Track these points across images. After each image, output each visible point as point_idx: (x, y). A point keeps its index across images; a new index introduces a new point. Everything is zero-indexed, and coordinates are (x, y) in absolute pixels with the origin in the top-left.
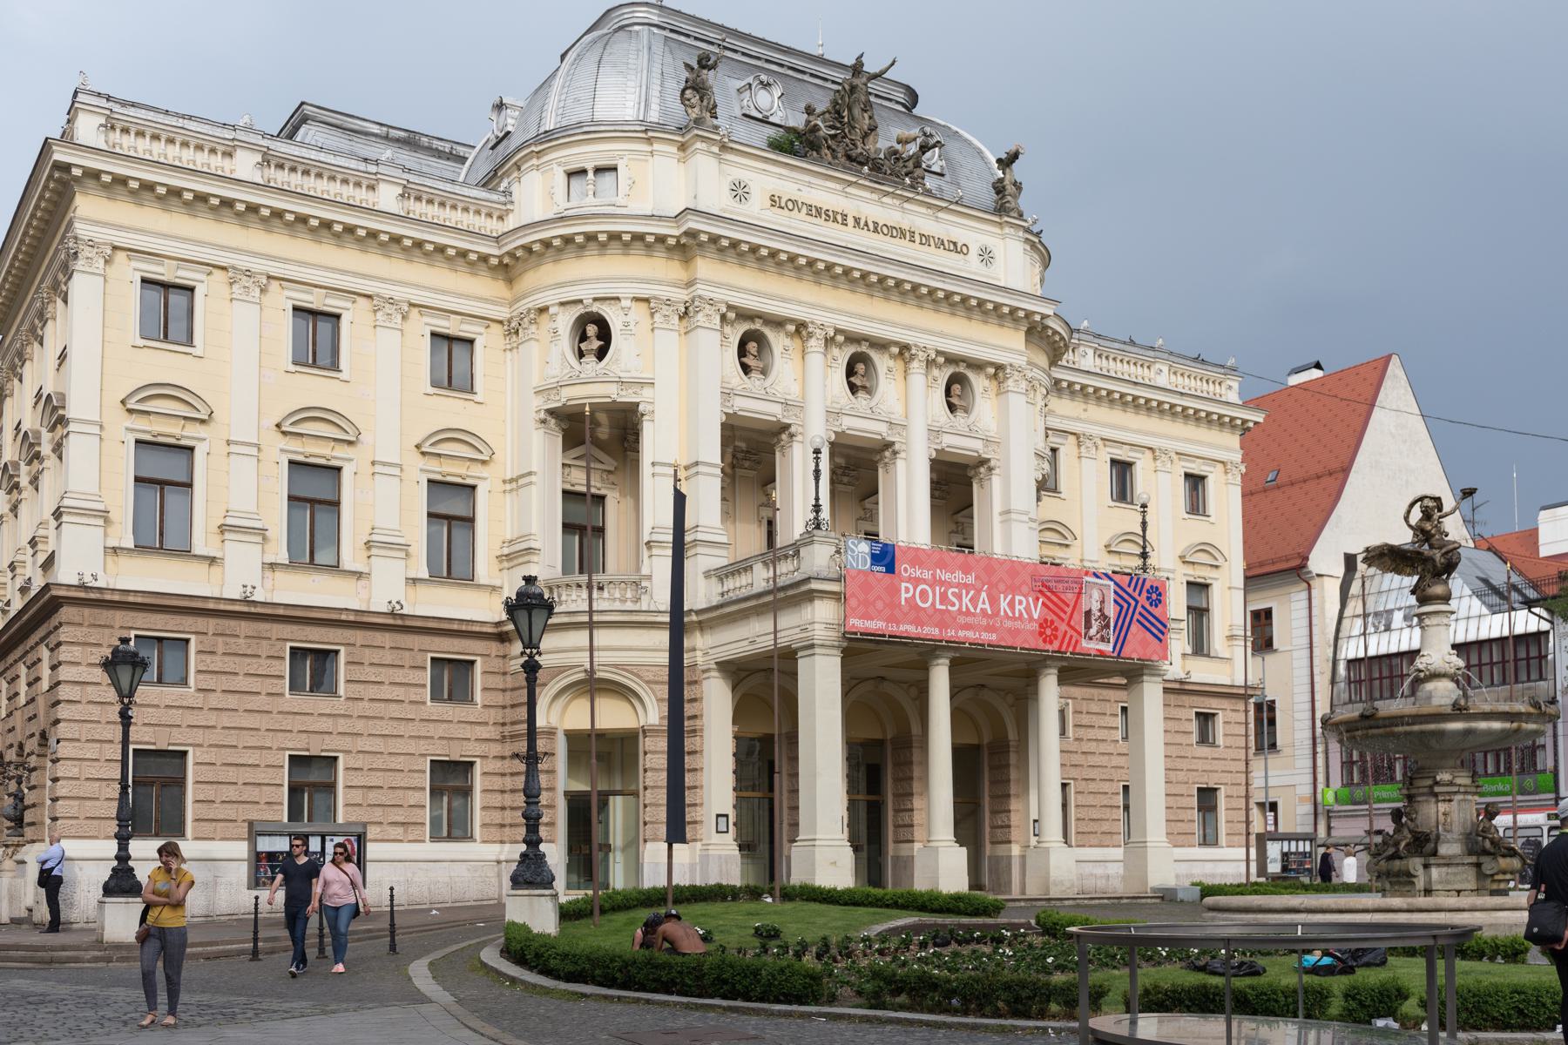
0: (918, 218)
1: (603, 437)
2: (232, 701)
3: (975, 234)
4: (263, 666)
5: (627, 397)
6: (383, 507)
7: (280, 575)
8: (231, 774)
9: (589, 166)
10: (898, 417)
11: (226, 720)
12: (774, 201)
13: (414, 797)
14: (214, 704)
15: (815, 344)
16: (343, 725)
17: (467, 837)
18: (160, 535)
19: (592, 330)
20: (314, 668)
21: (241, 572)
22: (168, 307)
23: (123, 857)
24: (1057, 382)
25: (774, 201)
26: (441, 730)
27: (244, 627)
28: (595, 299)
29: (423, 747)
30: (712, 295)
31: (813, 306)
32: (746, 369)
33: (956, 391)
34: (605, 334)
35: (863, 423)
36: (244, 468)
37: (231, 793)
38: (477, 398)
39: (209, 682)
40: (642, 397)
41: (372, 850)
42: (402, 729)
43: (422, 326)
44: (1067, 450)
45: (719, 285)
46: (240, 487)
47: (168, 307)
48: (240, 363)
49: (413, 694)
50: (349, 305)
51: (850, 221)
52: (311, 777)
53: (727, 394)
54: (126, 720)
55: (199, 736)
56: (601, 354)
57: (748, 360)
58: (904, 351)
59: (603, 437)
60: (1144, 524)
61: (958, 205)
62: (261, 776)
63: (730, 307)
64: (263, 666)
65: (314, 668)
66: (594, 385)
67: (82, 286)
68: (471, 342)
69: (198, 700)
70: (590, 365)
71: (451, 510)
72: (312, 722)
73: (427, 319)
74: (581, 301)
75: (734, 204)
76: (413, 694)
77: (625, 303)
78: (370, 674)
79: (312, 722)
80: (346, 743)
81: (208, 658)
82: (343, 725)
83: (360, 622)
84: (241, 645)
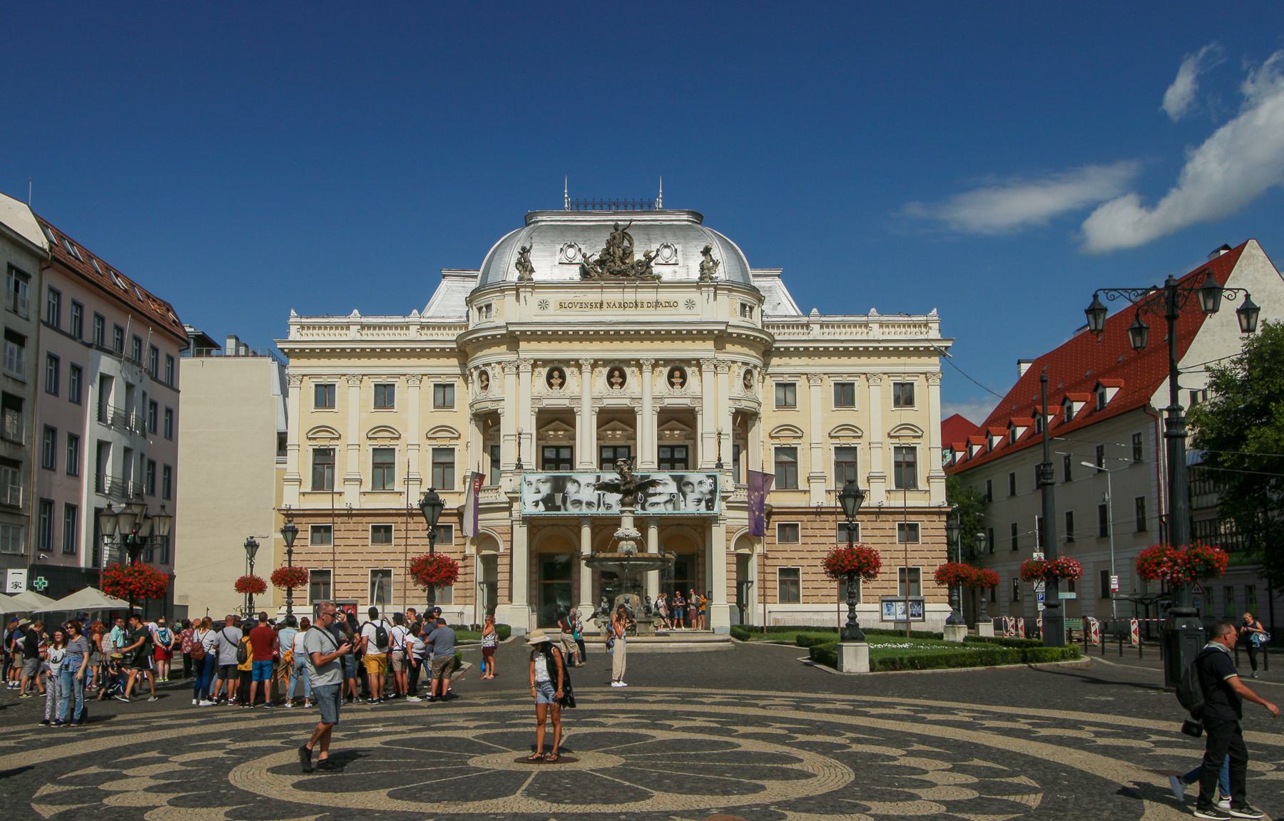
0: (647, 295)
4: (360, 534)
15: (586, 368)
20: (382, 533)
21: (351, 498)
23: (290, 611)
32: (551, 385)
36: (353, 456)
40: (500, 407)
43: (429, 384)
46: (353, 462)
51: (605, 305)
54: (290, 561)
58: (638, 364)
71: (443, 461)
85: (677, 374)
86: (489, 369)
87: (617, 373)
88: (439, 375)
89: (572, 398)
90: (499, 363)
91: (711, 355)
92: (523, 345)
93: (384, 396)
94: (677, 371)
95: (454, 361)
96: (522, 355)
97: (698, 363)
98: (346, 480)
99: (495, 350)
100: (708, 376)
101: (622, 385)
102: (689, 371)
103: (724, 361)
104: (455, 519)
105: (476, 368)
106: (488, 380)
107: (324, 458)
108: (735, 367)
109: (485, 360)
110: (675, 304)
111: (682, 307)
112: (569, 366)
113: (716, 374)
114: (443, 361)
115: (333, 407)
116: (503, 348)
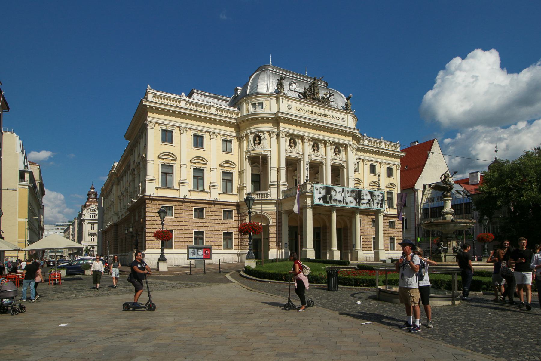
0: (328, 113)
1: (259, 163)
2: (182, 220)
3: (341, 116)
5: (265, 153)
6: (213, 177)
7: (191, 192)
8: (182, 235)
9: (257, 102)
10: (324, 156)
11: (181, 223)
12: (297, 109)
13: (220, 240)
16: (205, 224)
17: (232, 248)
18: (166, 184)
19: (257, 138)
20: (199, 213)
21: (184, 192)
22: (167, 136)
24: (358, 148)
25: (297, 109)
28: (258, 132)
29: (222, 229)
32: (291, 146)
33: (337, 151)
34: (260, 139)
37: (182, 239)
41: (213, 251)
42: (217, 225)
43: (220, 139)
44: (361, 162)
46: (183, 174)
47: (167, 136)
48: (183, 146)
49: (220, 218)
52: (199, 235)
53: (287, 152)
55: (175, 227)
56: (259, 144)
59: (259, 163)
60: (379, 179)
61: (336, 109)
62: (188, 235)
63: (288, 133)
65: (199, 213)
66: (258, 151)
67: (150, 132)
68: (231, 142)
69: (175, 220)
70: (258, 146)
71: (227, 177)
72: (199, 224)
74: (254, 133)
75: (288, 110)
76: (220, 218)
79: (199, 224)
80: (206, 228)
82: (205, 224)
83: (208, 203)
84: (184, 208)
86: (261, 134)
88: (226, 135)
89: (300, 154)
91: (351, 143)
92: (282, 125)
94: (338, 147)
95: (233, 129)
99: (265, 125)
104: (234, 208)
105: (251, 133)
109: (260, 130)
110: (336, 118)
111: (341, 120)
112: (298, 138)
114: (227, 128)
116: (270, 125)
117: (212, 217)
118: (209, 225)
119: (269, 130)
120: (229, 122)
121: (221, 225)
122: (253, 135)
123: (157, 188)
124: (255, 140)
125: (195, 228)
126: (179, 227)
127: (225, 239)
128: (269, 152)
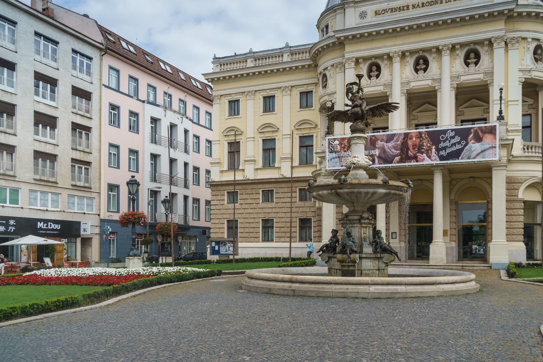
2: (247, 206)
7: (259, 171)
10: (435, 77)
11: (246, 211)
14: (243, 207)
20: (268, 196)
21: (249, 172)
26: (301, 209)
27: (251, 186)
28: (324, 70)
30: (349, 56)
31: (391, 46)
35: (421, 82)
38: (313, 108)
39: (242, 202)
45: (352, 52)
50: (276, 92)
56: (325, 87)
57: (371, 74)
58: (438, 51)
62: (254, 225)
64: (254, 196)
65: (268, 196)
68: (312, 92)
71: (306, 144)
72: (268, 210)
73: (298, 89)
77: (329, 68)
78: (281, 195)
81: (241, 196)
85: (472, 55)
86: (327, 73)
87: (421, 61)
89: (385, 85)
90: (333, 66)
91: (502, 33)
93: (269, 104)
96: (347, 56)
97: (490, 43)
98: (246, 161)
100: (499, 52)
101: (425, 70)
102: (483, 51)
103: (513, 39)
105: (320, 73)
106: (326, 81)
107: (234, 149)
108: (523, 44)
113: (507, 51)
115: (238, 114)
117: (282, 200)
118: (278, 210)
119: (332, 62)
120: (303, 67)
121: (256, 211)
122: (322, 75)
123: (222, 172)
124: (323, 82)
125: (262, 216)
126: (244, 216)
127: (301, 228)
128: (335, 96)
